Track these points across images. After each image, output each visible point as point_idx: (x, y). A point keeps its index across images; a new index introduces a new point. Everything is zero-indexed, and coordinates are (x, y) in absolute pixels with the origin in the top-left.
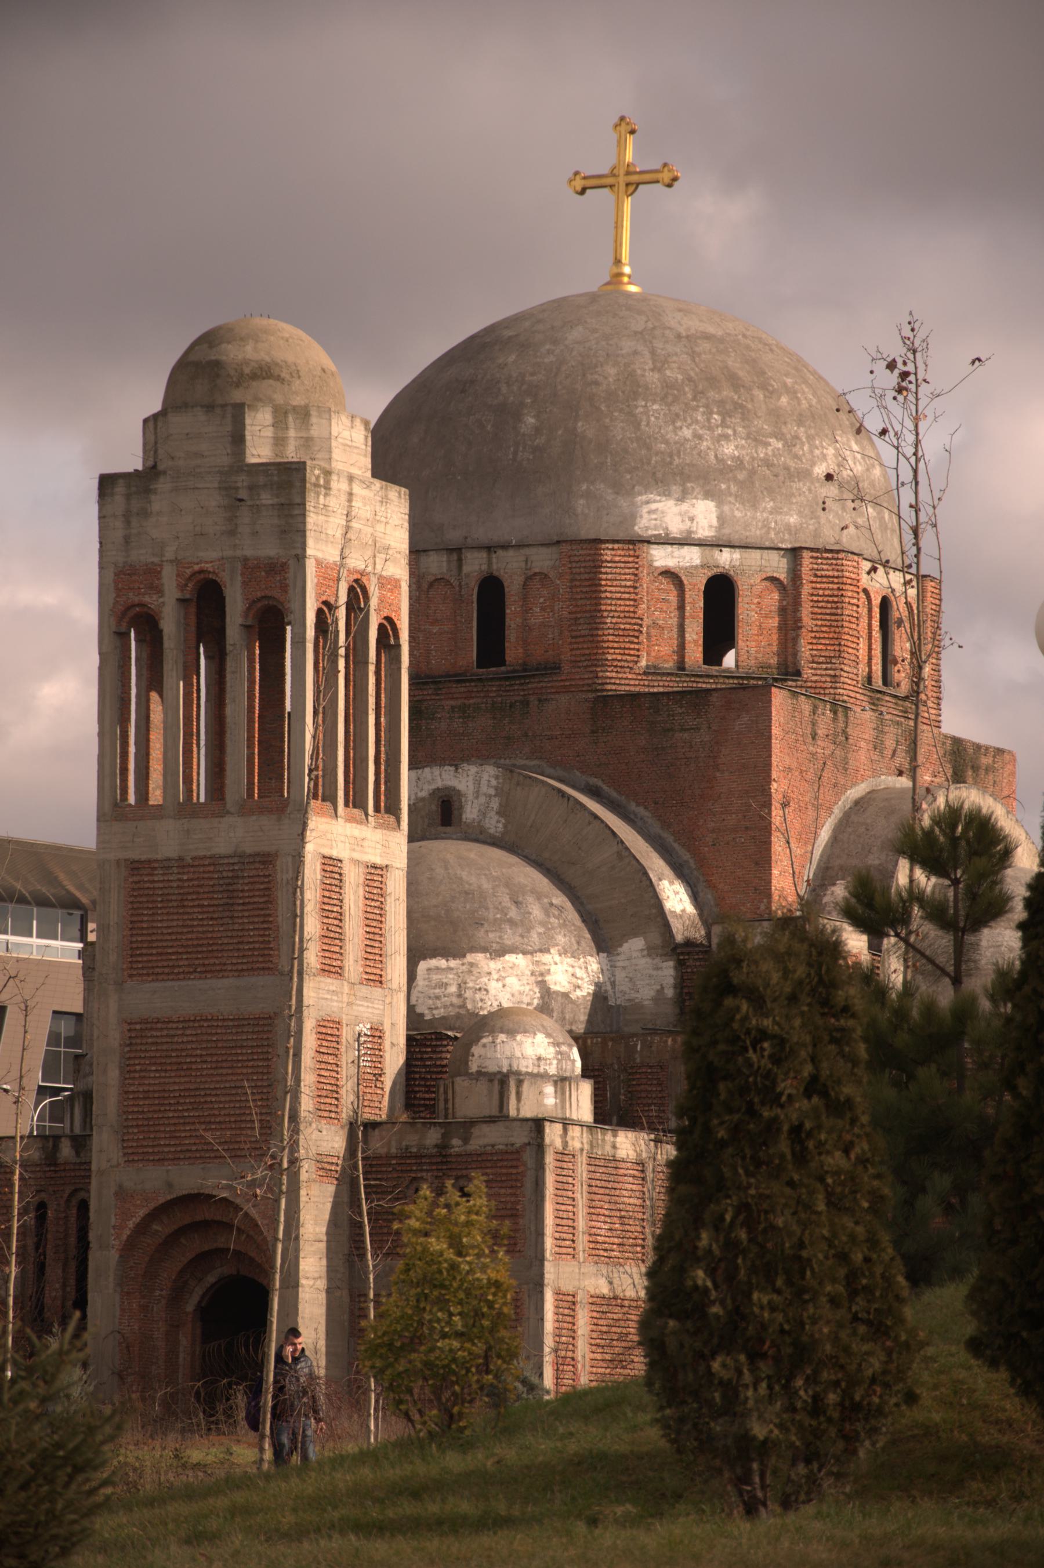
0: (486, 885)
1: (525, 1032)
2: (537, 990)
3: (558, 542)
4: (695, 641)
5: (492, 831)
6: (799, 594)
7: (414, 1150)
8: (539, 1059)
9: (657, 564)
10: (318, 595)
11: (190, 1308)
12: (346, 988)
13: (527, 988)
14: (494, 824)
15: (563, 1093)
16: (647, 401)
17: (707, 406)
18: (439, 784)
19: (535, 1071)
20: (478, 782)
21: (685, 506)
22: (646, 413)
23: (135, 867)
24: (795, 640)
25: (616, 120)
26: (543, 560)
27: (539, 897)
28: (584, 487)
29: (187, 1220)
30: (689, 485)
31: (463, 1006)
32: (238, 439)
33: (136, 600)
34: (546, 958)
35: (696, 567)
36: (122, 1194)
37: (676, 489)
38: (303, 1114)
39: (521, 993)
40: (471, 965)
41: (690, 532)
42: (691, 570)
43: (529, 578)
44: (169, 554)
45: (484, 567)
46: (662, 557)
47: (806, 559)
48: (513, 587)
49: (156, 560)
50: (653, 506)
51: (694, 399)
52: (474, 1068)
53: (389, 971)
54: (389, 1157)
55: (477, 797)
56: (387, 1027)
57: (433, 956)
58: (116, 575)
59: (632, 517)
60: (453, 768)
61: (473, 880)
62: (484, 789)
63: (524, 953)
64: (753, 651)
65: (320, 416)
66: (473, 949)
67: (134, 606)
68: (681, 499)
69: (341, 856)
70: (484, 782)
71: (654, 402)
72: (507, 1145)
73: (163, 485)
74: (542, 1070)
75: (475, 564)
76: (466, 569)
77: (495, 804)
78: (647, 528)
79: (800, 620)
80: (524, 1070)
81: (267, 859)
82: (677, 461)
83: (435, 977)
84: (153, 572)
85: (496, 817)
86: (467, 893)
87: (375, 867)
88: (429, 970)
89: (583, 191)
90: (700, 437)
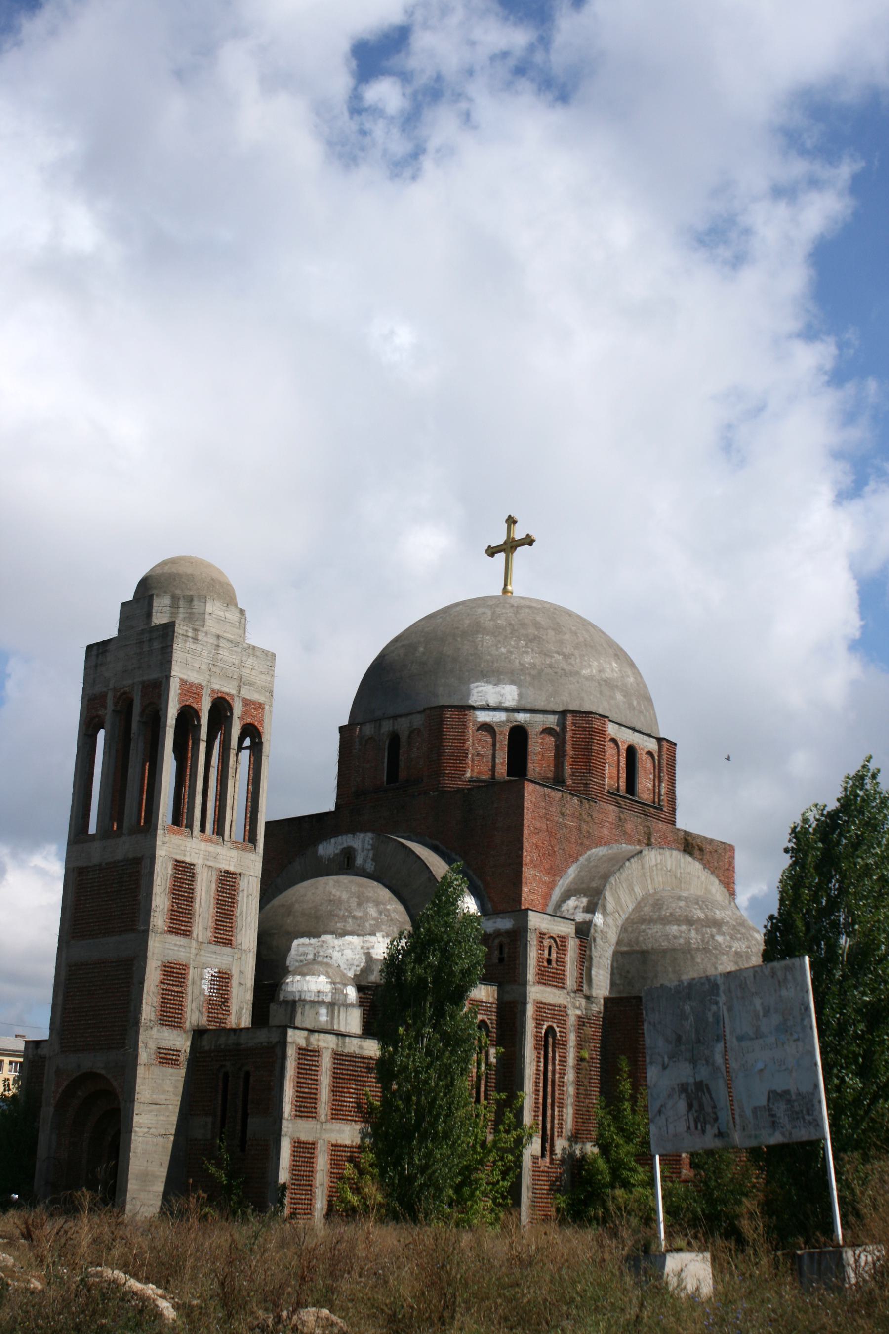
0: (345, 896)
1: (313, 974)
2: (364, 958)
3: (425, 710)
4: (502, 764)
5: (368, 870)
6: (564, 738)
7: (223, 1047)
9: (479, 720)
10: (180, 701)
12: (194, 944)
13: (357, 956)
14: (370, 866)
15: (333, 1013)
16: (483, 634)
18: (345, 845)
19: (316, 999)
20: (363, 843)
21: (498, 689)
22: (482, 641)
24: (563, 763)
25: (507, 518)
26: (418, 721)
27: (377, 903)
28: (443, 681)
30: (502, 677)
34: (372, 939)
35: (503, 722)
37: (492, 679)
38: (143, 1021)
39: (353, 959)
40: (323, 942)
41: (501, 703)
42: (501, 724)
43: (412, 732)
45: (391, 729)
46: (483, 717)
47: (569, 718)
48: (404, 738)
49: (105, 689)
50: (480, 689)
51: (511, 633)
52: (281, 998)
53: (239, 937)
55: (362, 851)
56: (235, 972)
57: (302, 937)
58: (88, 701)
59: (468, 694)
60: (351, 836)
61: (338, 894)
63: (358, 935)
64: (537, 769)
65: (199, 601)
68: (496, 685)
69: (194, 861)
70: (366, 842)
71: (488, 635)
72: (268, 1043)
74: (320, 999)
75: (387, 727)
76: (382, 731)
77: (371, 855)
78: (476, 701)
79: (565, 751)
80: (308, 998)
82: (496, 665)
86: (331, 901)
87: (227, 872)
88: (298, 945)
90: (511, 652)
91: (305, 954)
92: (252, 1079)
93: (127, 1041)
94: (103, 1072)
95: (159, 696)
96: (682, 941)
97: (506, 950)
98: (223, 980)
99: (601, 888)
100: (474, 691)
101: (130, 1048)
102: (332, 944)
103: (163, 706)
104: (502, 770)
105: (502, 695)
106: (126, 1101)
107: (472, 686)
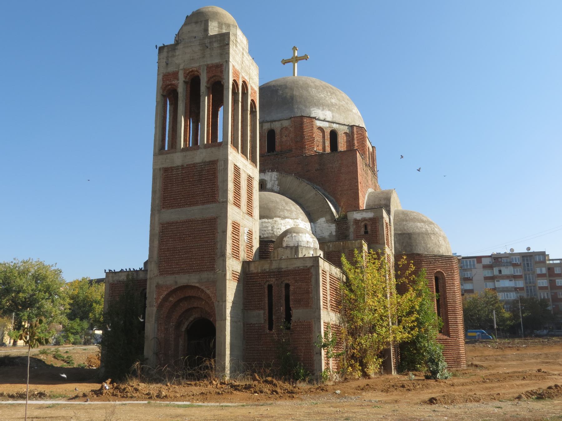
3: (291, 118)
8: (308, 242)
9: (317, 125)
11: (183, 330)
14: (276, 188)
17: (326, 91)
19: (307, 246)
21: (323, 112)
23: (166, 170)
25: (293, 47)
26: (286, 123)
29: (182, 296)
30: (324, 107)
31: (273, 234)
32: (206, 30)
33: (170, 83)
34: (297, 221)
35: (327, 127)
36: (158, 286)
37: (321, 108)
38: (227, 254)
40: (276, 221)
42: (326, 128)
43: (282, 129)
44: (181, 67)
46: (319, 124)
48: (277, 131)
49: (177, 70)
50: (316, 111)
52: (284, 245)
54: (257, 273)
57: (264, 218)
58: (163, 76)
59: (310, 113)
60: (263, 174)
62: (273, 179)
63: (291, 219)
65: (233, 27)
66: (276, 217)
67: (169, 85)
70: (273, 177)
71: (313, 88)
72: (304, 267)
73: (180, 47)
74: (309, 246)
76: (264, 128)
77: (277, 183)
79: (354, 143)
80: (303, 245)
81: (214, 163)
82: (321, 101)
83: (264, 224)
84: (175, 75)
85: (277, 186)
89: (284, 64)
91: (267, 227)
92: (291, 288)
93: (215, 266)
94: (197, 285)
95: (222, 72)
96: (424, 229)
97: (369, 228)
98: (250, 233)
99: (388, 204)
100: (313, 112)
101: (219, 270)
102: (280, 223)
103: (225, 77)
104: (328, 150)
105: (326, 115)
106: (218, 302)
107: (311, 109)
